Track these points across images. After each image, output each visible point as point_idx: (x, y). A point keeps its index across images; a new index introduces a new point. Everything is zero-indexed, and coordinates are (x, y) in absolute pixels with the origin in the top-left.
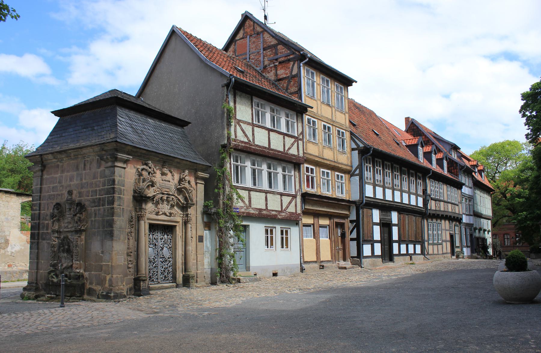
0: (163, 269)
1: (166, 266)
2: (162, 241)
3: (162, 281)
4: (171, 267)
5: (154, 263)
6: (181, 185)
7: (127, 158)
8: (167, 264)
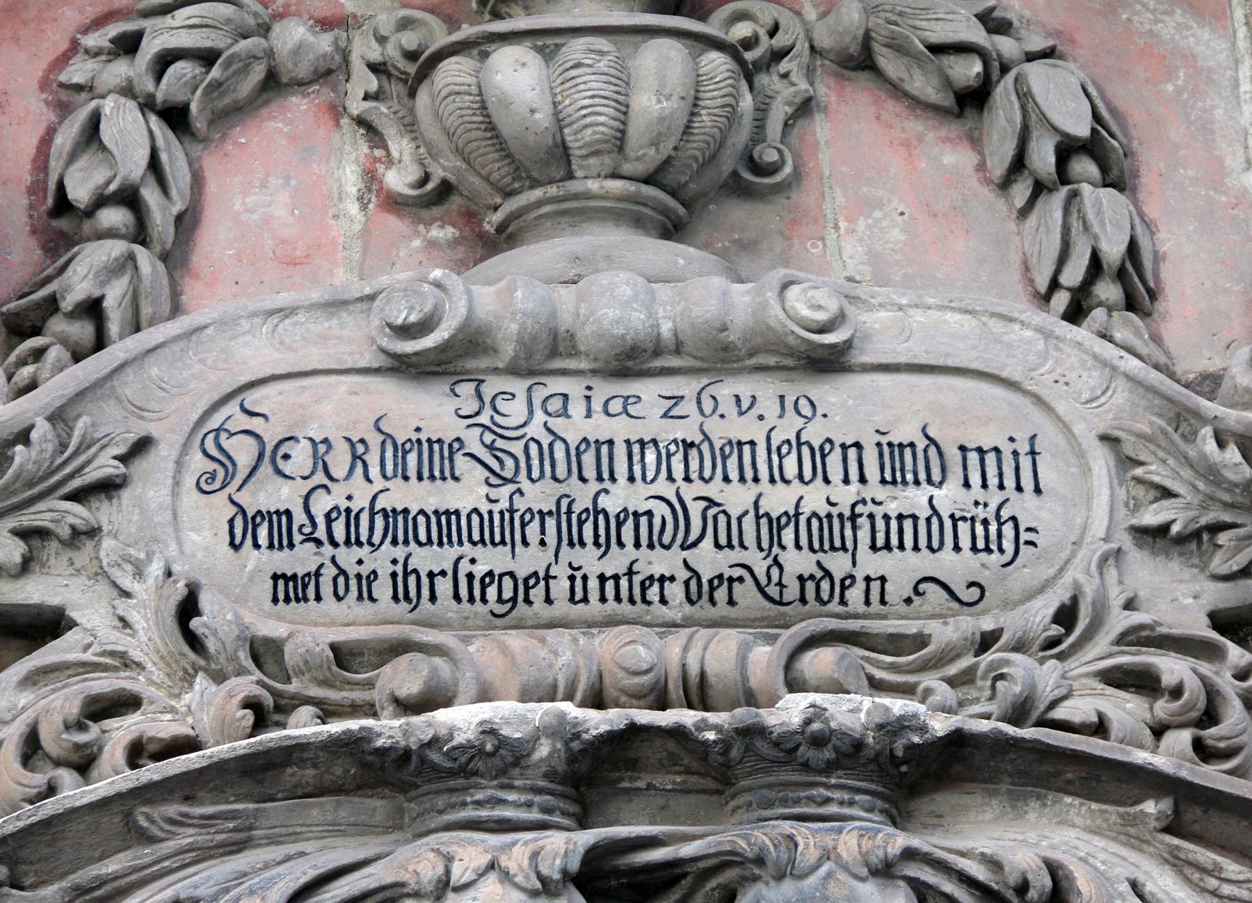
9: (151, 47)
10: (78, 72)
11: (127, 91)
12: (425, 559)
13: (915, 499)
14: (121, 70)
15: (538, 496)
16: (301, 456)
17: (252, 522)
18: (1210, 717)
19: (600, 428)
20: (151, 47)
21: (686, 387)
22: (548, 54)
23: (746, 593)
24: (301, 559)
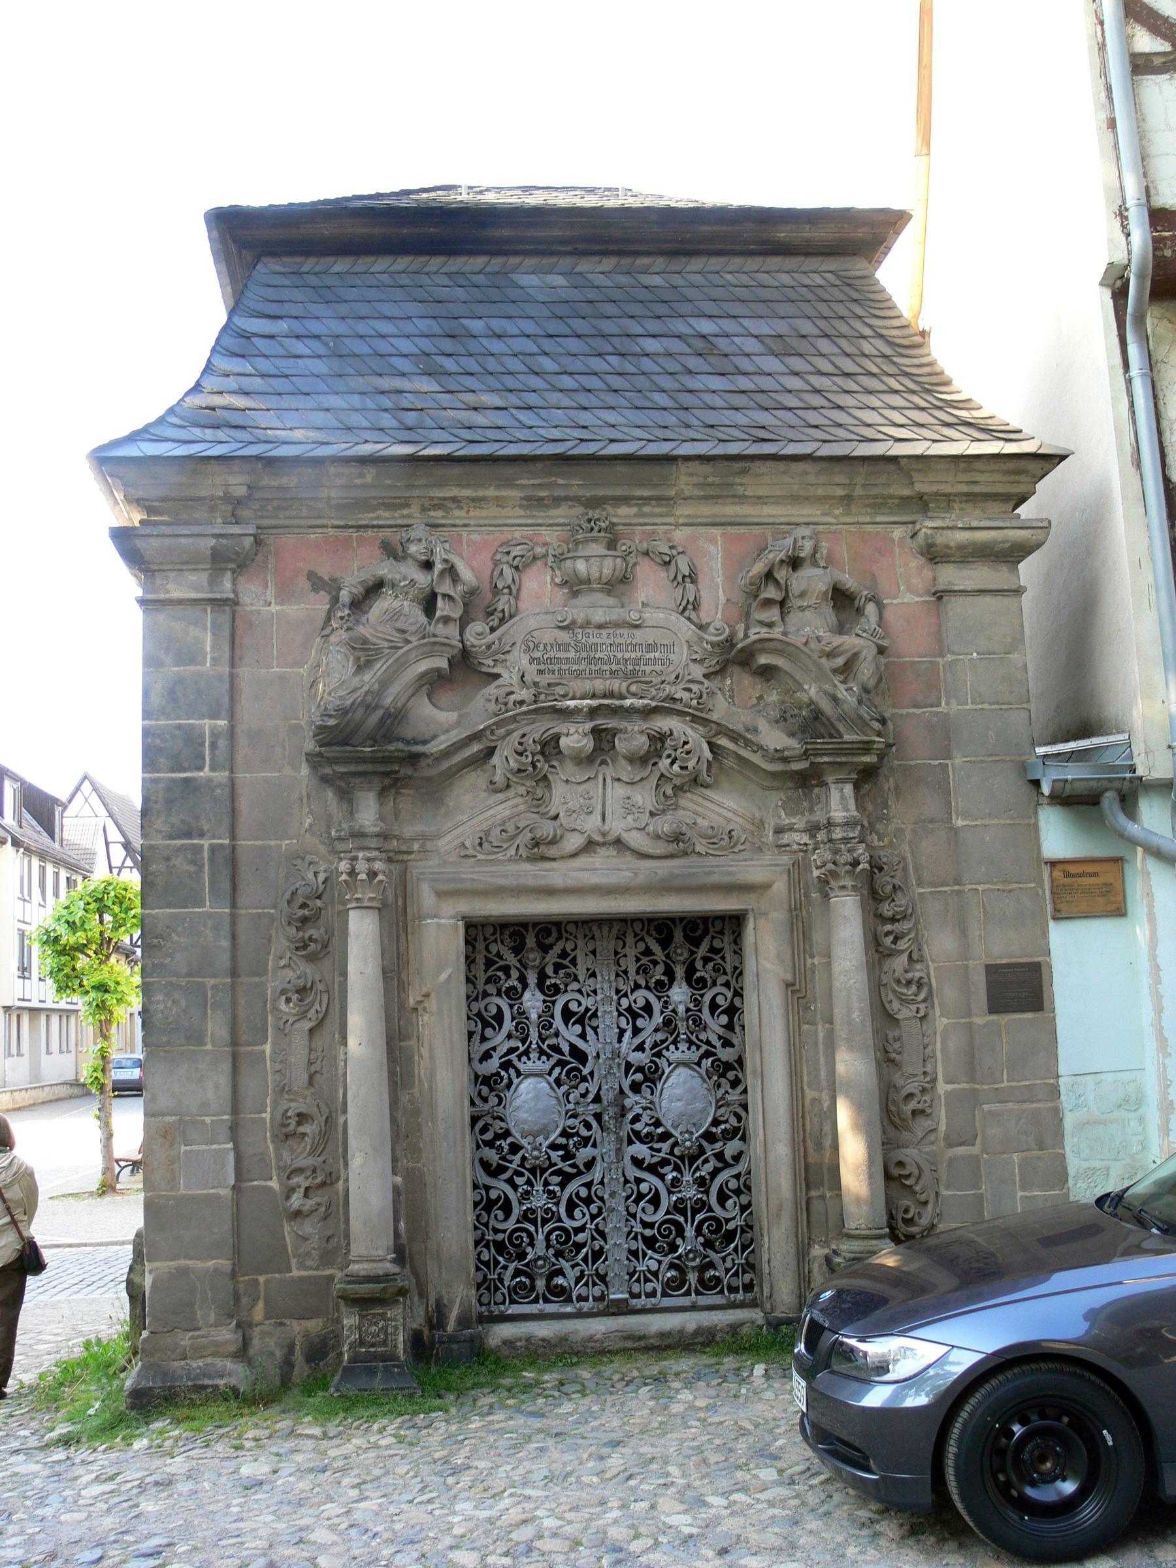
0: (660, 1216)
2: (648, 1025)
3: (653, 1294)
5: (566, 1179)
9: (513, 554)
10: (498, 557)
11: (508, 563)
12: (563, 667)
13: (652, 655)
14: (506, 558)
15: (584, 655)
16: (541, 647)
18: (701, 697)
19: (595, 640)
20: (513, 554)
21: (611, 631)
22: (587, 561)
23: (621, 673)
24: (542, 667)
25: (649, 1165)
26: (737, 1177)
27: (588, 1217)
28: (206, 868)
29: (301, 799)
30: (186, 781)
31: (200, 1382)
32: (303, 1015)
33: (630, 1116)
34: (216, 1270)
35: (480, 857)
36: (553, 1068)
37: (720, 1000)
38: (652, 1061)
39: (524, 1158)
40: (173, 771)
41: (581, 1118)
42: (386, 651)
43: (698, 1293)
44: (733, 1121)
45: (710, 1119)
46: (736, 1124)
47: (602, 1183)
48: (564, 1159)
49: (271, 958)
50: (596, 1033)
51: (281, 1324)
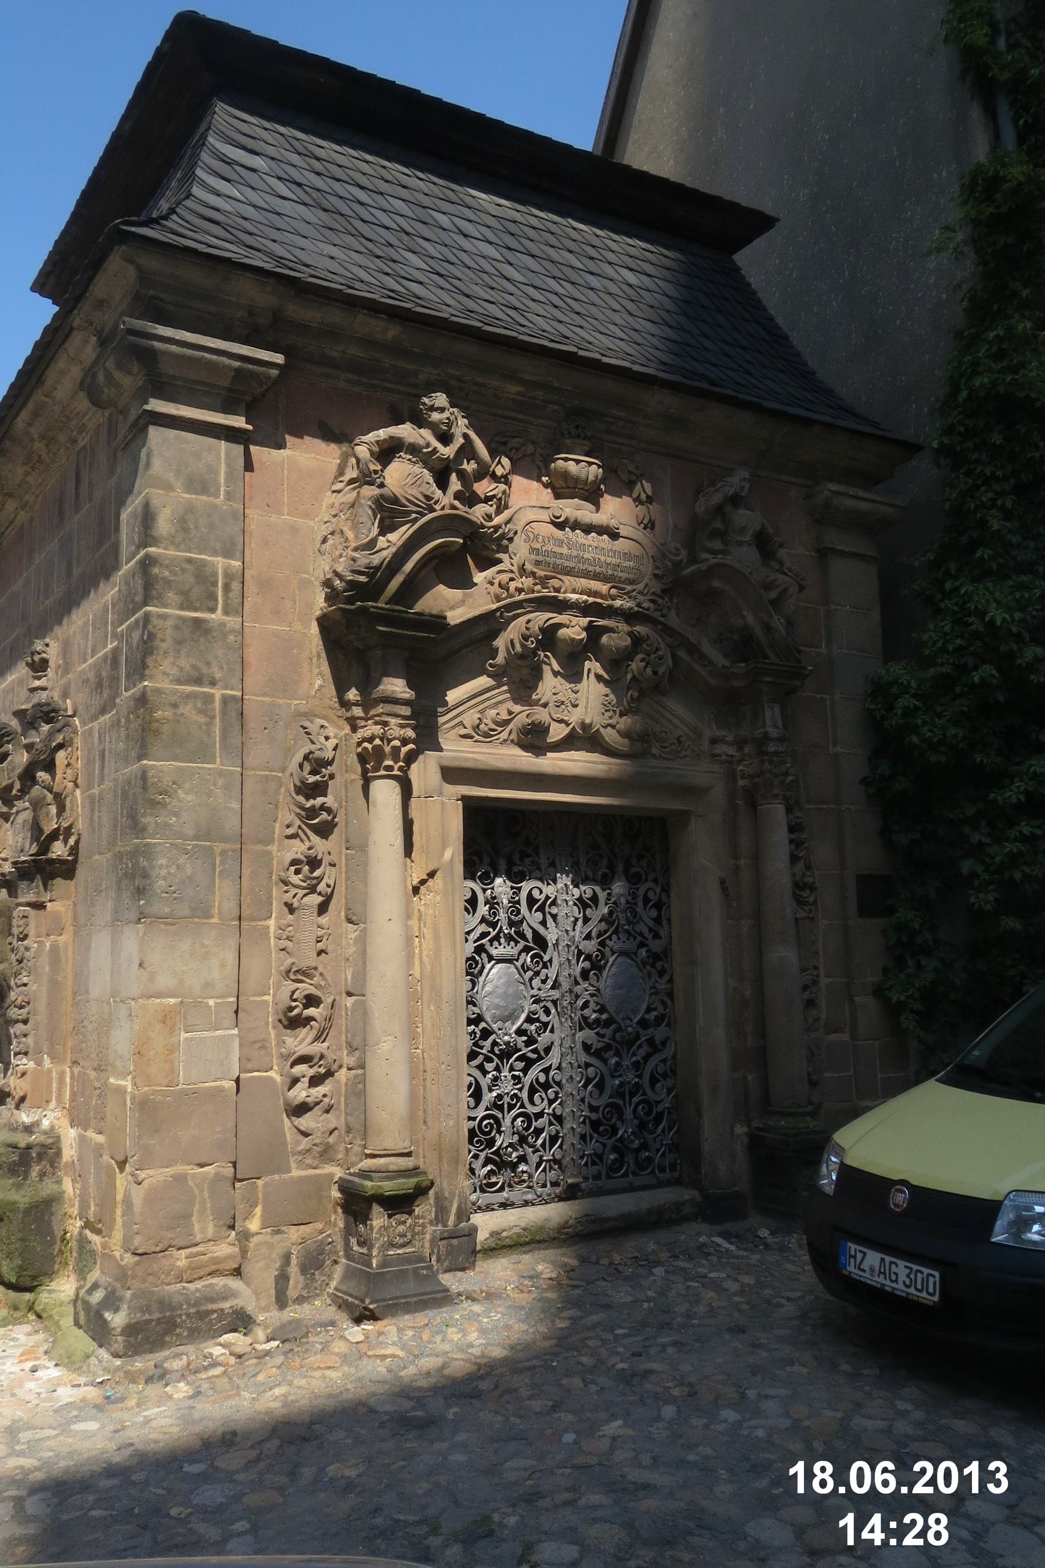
0: (605, 1099)
1: (631, 1077)
4: (670, 1082)
5: (529, 1063)
6: (704, 556)
7: (237, 364)
8: (637, 1065)
9: (510, 445)
15: (575, 553)
17: (533, 549)
24: (540, 558)
25: (596, 1050)
26: (664, 1061)
27: (546, 1102)
28: (218, 720)
29: (311, 659)
30: (197, 622)
31: (204, 1308)
32: (312, 889)
33: (580, 1002)
34: (217, 1174)
35: (477, 737)
36: (519, 954)
37: (651, 895)
38: (598, 950)
39: (495, 1043)
40: (182, 607)
41: (542, 1004)
42: (414, 515)
43: (634, 1174)
44: (660, 1008)
45: (644, 1007)
46: (663, 1012)
47: (559, 1068)
48: (528, 1044)
49: (277, 825)
50: (555, 921)
51: (278, 1232)
